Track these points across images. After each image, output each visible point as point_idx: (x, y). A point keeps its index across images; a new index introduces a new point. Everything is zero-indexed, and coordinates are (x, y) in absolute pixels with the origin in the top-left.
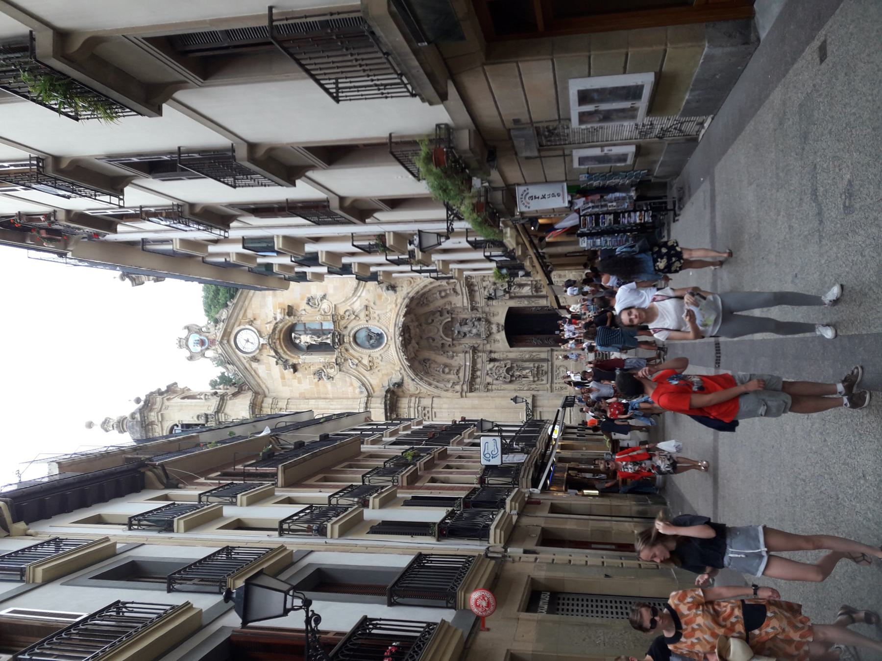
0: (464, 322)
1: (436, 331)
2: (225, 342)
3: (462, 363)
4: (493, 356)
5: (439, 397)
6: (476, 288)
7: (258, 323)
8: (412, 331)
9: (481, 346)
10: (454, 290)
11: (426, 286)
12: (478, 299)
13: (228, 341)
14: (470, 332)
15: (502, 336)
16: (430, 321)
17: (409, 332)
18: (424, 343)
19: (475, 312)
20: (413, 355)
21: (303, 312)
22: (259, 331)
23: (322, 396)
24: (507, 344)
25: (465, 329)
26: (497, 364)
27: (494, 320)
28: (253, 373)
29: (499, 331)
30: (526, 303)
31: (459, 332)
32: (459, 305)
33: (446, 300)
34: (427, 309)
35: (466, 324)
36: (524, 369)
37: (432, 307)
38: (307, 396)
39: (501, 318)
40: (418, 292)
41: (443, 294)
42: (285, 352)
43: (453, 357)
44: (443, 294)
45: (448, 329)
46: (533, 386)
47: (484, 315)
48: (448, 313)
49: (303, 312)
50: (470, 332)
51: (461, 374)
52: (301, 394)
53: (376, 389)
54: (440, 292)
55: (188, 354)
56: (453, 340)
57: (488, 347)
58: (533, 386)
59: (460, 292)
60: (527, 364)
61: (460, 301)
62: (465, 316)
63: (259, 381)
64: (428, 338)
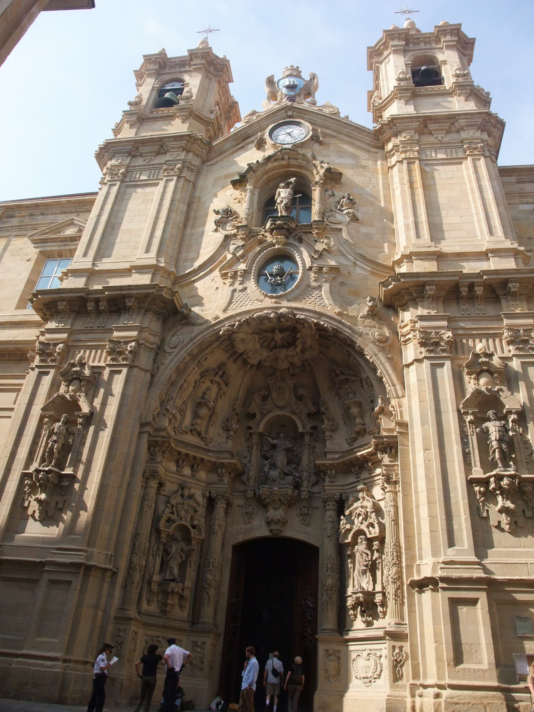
0: (293, 460)
1: (281, 403)
2: (290, 113)
3: (211, 446)
4: (221, 506)
5: (151, 383)
7: (316, 146)
8: (284, 353)
9: (243, 488)
13: (290, 117)
14: (274, 466)
15: (259, 529)
16: (301, 392)
17: (283, 346)
19: (313, 479)
20: (240, 348)
21: (330, 192)
22: (302, 143)
23: (190, 222)
24: (241, 538)
25: (280, 458)
26: (202, 510)
28: (239, 146)
29: (268, 523)
30: (329, 582)
31: (274, 447)
32: (329, 445)
33: (341, 422)
35: (289, 463)
36: (183, 566)
37: (328, 397)
38: (194, 206)
42: (267, 172)
43: (228, 430)
46: (137, 577)
47: (304, 495)
48: (314, 428)
49: (330, 192)
50: (274, 466)
51: (190, 438)
52: (199, 198)
53: (186, 289)
55: (276, 80)
56: (261, 435)
57: (238, 501)
58: (137, 577)
60: (191, 573)
62: (305, 459)
63: (227, 153)
64: (268, 388)
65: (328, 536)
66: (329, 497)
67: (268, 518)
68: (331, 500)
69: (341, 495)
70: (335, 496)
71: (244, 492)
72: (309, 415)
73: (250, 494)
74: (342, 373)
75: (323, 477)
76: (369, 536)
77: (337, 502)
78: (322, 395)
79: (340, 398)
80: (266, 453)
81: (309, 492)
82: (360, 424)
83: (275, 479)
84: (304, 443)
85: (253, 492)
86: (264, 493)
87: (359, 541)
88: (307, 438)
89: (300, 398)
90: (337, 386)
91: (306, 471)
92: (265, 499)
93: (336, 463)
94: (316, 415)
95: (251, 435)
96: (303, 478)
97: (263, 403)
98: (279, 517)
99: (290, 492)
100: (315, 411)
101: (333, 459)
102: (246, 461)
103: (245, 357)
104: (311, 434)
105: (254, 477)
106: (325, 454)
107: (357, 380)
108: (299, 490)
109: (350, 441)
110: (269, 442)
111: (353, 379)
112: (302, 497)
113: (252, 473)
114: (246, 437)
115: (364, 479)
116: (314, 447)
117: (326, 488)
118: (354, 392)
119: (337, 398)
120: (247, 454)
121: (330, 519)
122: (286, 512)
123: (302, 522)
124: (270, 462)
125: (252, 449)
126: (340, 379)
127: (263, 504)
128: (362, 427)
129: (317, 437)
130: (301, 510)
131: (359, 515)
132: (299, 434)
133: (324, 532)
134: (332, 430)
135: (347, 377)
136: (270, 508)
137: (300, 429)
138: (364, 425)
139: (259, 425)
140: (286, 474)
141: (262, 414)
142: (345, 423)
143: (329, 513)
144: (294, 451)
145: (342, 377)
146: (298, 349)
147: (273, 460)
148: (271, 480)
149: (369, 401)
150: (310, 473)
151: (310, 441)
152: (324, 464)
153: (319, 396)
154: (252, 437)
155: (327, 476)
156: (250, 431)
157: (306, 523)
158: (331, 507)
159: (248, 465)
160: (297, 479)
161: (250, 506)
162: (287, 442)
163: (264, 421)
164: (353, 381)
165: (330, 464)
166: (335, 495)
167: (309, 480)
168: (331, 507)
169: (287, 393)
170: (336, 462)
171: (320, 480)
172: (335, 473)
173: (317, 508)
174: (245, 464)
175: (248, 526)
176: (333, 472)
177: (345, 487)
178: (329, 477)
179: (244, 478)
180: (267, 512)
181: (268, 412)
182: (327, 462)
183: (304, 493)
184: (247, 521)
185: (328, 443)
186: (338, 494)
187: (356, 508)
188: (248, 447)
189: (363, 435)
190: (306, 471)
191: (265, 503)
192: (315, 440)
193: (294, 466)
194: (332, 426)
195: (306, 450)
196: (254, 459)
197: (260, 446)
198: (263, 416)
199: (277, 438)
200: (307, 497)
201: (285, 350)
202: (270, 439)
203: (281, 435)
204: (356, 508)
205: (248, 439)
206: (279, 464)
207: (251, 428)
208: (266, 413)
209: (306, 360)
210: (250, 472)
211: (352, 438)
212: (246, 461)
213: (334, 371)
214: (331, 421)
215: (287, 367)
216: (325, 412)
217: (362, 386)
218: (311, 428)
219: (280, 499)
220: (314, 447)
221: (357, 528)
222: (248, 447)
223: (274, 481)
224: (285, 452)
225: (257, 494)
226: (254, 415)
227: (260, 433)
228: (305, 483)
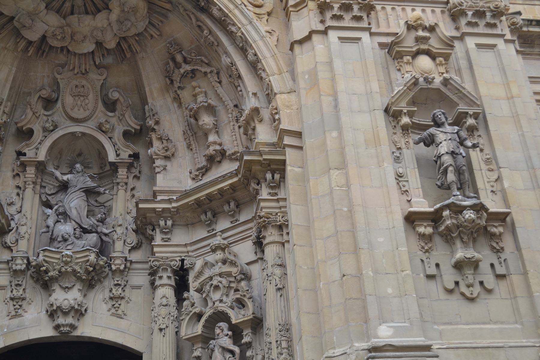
6: (223, 224)
8: (86, 24)
10: (213, 160)
11: (243, 47)
12: (180, 237)
14: (64, 216)
18: (41, 73)
19: (133, 239)
25: (75, 203)
27: (98, 302)
29: (52, 314)
32: (162, 182)
34: (153, 84)
37: (159, 102)
39: (99, 325)
40: (223, 23)
41: (206, 120)
44: (206, 120)
45: (79, 152)
48: (135, 156)
50: (64, 216)
54: (211, 110)
56: (41, 167)
59: (207, 179)
61: (176, 178)
64: (56, 85)
65: (161, 330)
66: (162, 265)
67: (52, 305)
68: (165, 270)
69: (182, 261)
70: (173, 263)
71: (8, 262)
72: (126, 135)
73: (20, 265)
74: (185, 61)
75: (150, 232)
76: (234, 322)
77: (175, 272)
78: (150, 100)
79: (180, 105)
80: (50, 198)
81: (126, 259)
82: (215, 143)
83: (67, 236)
84: (118, 181)
85: (25, 261)
86: (46, 262)
87: (218, 331)
88: (122, 172)
89: (111, 106)
90: (177, 85)
91: (120, 225)
92: (46, 272)
93: (173, 208)
94: (139, 135)
95: (24, 166)
96: (115, 237)
97: (46, 113)
98: (72, 302)
99: (92, 257)
100: (138, 128)
101: (170, 201)
102: (12, 210)
103: (16, 23)
104: (130, 166)
105: (27, 236)
106: (155, 196)
107: (211, 72)
108: (107, 257)
109: (197, 173)
110: (57, 178)
111: (203, 70)
112: (114, 268)
113: (22, 230)
114: (13, 171)
115: (223, 232)
116: (133, 189)
117: (155, 249)
118: (206, 93)
119: (176, 105)
120: (15, 198)
121: (164, 301)
122: (85, 296)
123: (113, 310)
124: (56, 210)
125: (24, 191)
126: (182, 71)
127: (44, 281)
128: (218, 148)
129: (140, 172)
130: (111, 291)
131: (217, 288)
132: (108, 168)
133: (154, 323)
134: (167, 158)
135: (195, 67)
136: (56, 287)
137: (112, 157)
138: (220, 145)
139: (37, 149)
140: (85, 231)
141: (45, 130)
142: (189, 147)
143: (160, 292)
144: (99, 194)
145: (188, 68)
146: (114, 17)
147: (63, 206)
148: (60, 239)
149: (232, 105)
150: (127, 228)
151: (128, 178)
152: (154, 209)
153: (144, 101)
154: (25, 170)
155: (158, 230)
156: (23, 158)
157: (120, 312)
158: (165, 281)
159: (16, 217)
160: (104, 238)
161: (20, 285)
162: (88, 179)
163: (48, 143)
164: (205, 73)
165: (163, 209)
166: (171, 261)
167: (125, 241)
168: (165, 281)
169: (91, 97)
170: (174, 205)
171: (143, 241)
172: (172, 225)
173: (139, 287)
174: (12, 215)
175: (16, 321)
176: (169, 223)
177: (189, 248)
178: (162, 232)
179: (9, 238)
180: (50, 295)
181: (56, 127)
182: (160, 206)
183: (118, 262)
184: (13, 313)
185: (159, 177)
186: (178, 259)
187: (211, 278)
188: (18, 187)
189: (220, 162)
190: (120, 225)
191: (47, 278)
192: (135, 177)
193: (99, 216)
194: (166, 150)
195: (121, 193)
196: (27, 207)
197: (38, 187)
198: (46, 134)
199: (71, 172)
200: (122, 267)
201: (90, 17)
202: (58, 173)
203: (78, 166)
204: (211, 278)
205: (18, 175)
206: (74, 213)
207: (25, 154)
208: (51, 128)
209: (124, 38)
210: (20, 228)
211: (202, 168)
212: (12, 210)
213: (174, 59)
214: (165, 142)
215: (91, 50)
216: (155, 127)
217: (220, 82)
218: (130, 156)
219: (74, 272)
220: (133, 189)
221: (212, 311)
222: (18, 187)
223: (65, 240)
224: (84, 194)
225: (34, 264)
226: (30, 133)
227: (38, 162)
228: (119, 246)
